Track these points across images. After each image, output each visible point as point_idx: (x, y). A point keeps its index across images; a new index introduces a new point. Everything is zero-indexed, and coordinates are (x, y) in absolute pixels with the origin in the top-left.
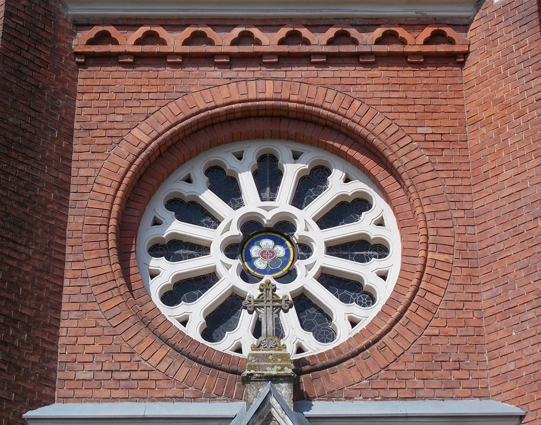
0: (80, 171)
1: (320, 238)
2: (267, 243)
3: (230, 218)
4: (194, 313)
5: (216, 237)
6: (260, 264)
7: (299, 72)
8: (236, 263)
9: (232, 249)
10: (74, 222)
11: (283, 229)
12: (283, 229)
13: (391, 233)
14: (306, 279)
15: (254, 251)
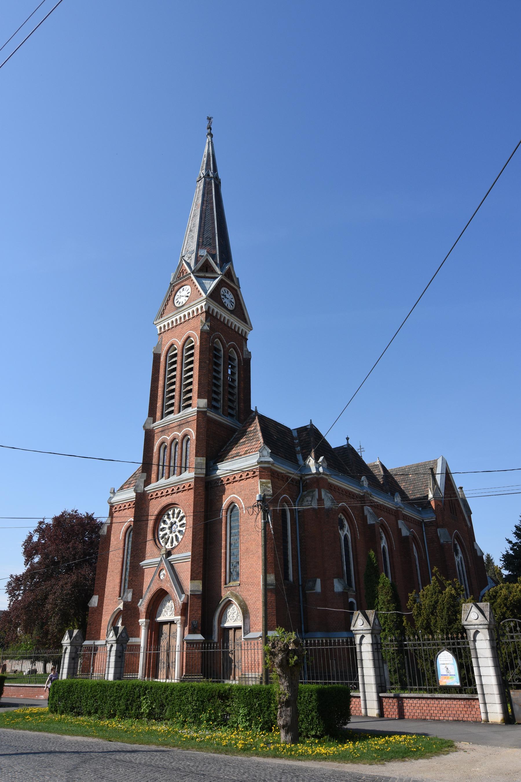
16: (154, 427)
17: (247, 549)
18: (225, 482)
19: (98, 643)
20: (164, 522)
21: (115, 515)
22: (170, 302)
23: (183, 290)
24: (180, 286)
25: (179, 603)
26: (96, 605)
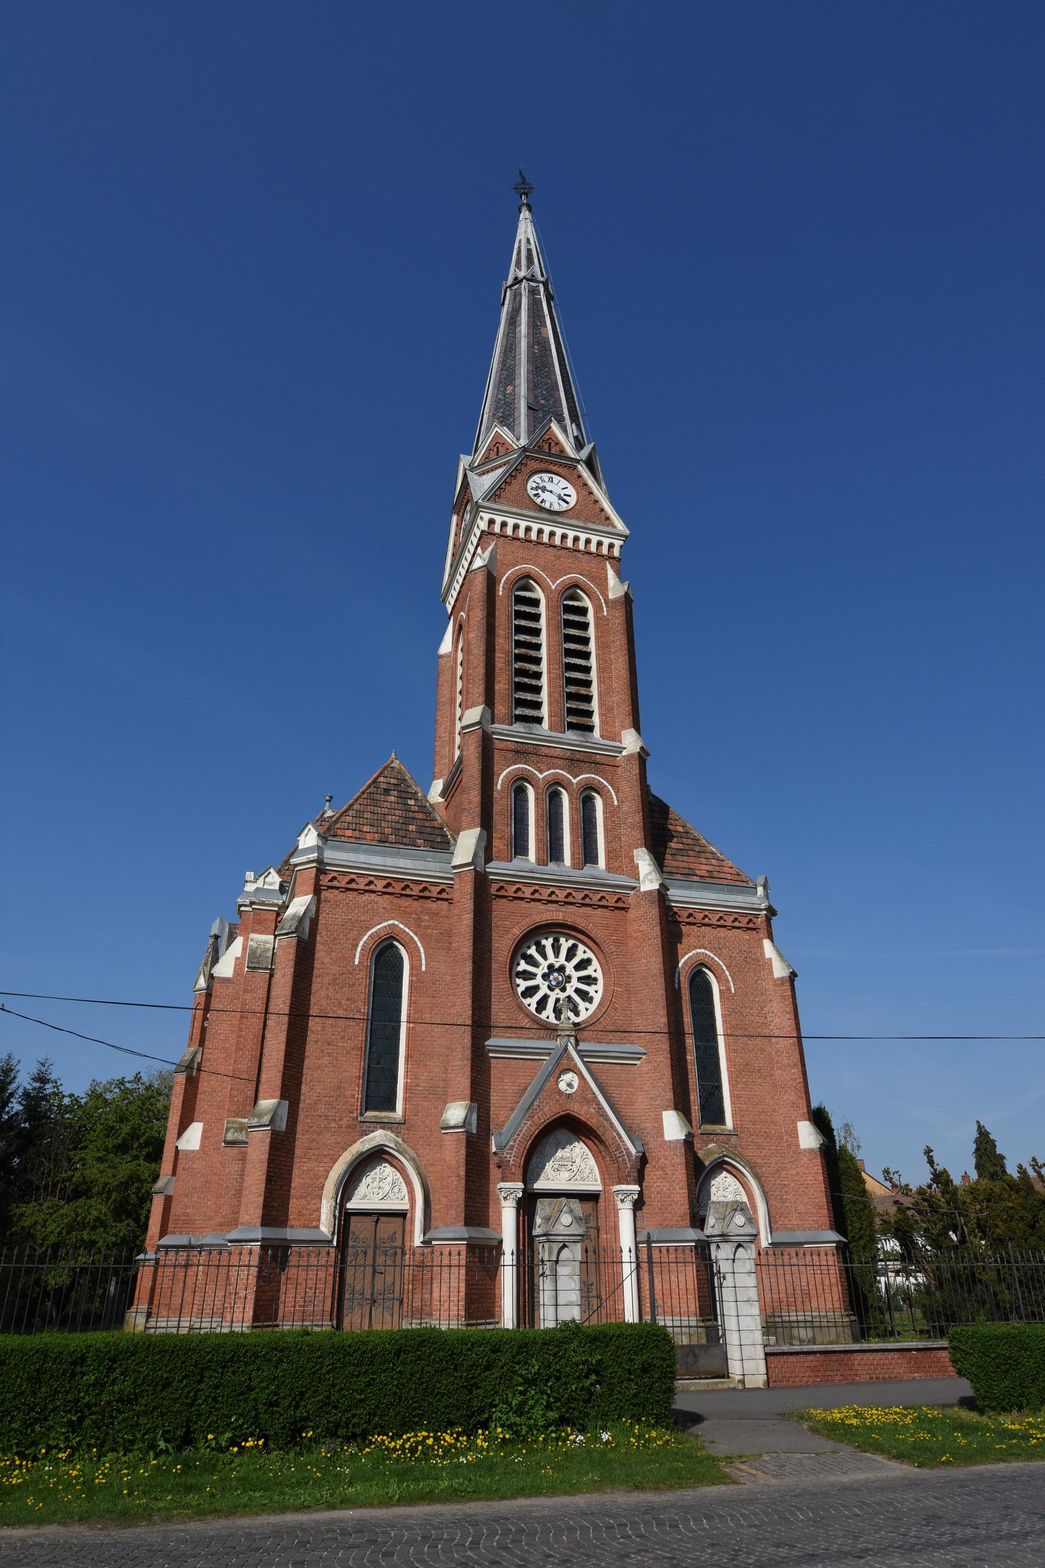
0: (495, 945)
1: (576, 975)
2: (556, 974)
3: (544, 965)
4: (532, 1002)
5: (539, 972)
6: (554, 983)
7: (571, 909)
8: (547, 983)
9: (545, 977)
10: (494, 966)
11: (562, 969)
12: (562, 969)
13: (599, 975)
14: (570, 991)
15: (551, 978)
16: (494, 733)
17: (747, 1065)
18: (683, 916)
19: (290, 1234)
20: (531, 961)
21: (325, 894)
22: (516, 485)
23: (551, 480)
24: (543, 466)
25: (629, 1154)
26: (284, 1127)
